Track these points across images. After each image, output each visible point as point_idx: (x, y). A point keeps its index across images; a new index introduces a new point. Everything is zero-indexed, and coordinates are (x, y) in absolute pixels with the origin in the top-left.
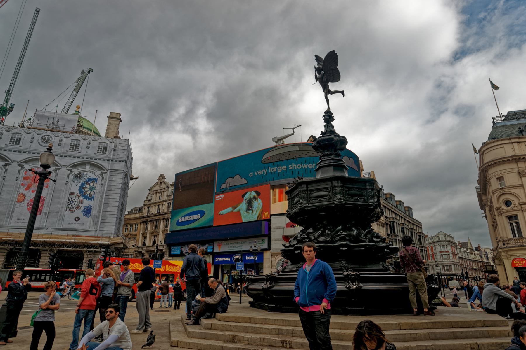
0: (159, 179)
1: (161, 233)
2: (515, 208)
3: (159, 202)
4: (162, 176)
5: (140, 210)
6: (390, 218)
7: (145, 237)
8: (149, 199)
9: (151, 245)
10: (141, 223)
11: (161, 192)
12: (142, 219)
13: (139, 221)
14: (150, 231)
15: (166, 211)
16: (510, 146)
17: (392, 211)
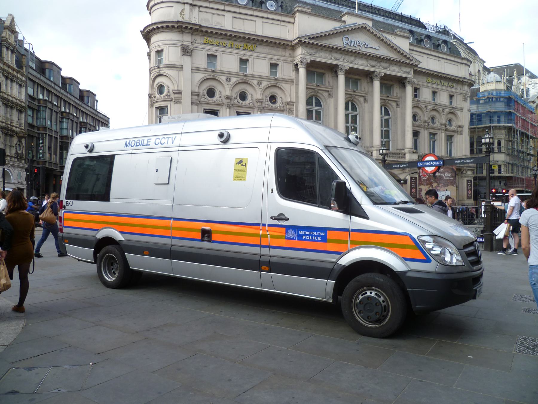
2: (166, 97)
6: (39, 100)
16: (181, 7)
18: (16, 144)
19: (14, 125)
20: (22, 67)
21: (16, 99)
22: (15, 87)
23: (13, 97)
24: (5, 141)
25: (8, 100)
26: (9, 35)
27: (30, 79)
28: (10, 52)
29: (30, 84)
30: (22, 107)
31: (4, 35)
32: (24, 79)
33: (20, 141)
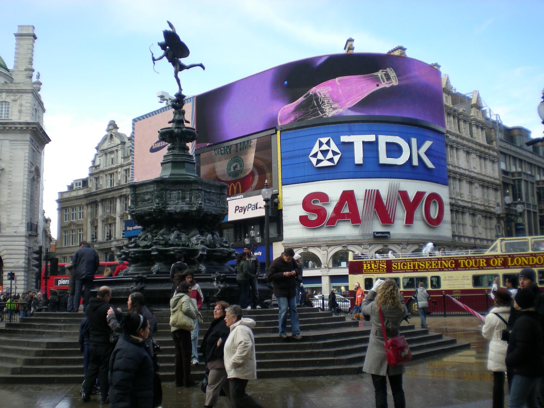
0: (108, 130)
1: (118, 220)
3: (111, 169)
4: (113, 125)
5: (85, 182)
6: (513, 174)
7: (96, 227)
8: (97, 163)
9: (105, 240)
10: (87, 205)
11: (112, 152)
12: (89, 198)
13: (84, 202)
14: (102, 216)
15: (123, 183)
17: (521, 161)
18: (496, 226)
19: (492, 205)
20: (492, 141)
21: (491, 178)
22: (489, 164)
23: (488, 177)
24: (486, 224)
25: (483, 181)
26: (477, 112)
27: (501, 153)
28: (480, 130)
29: (502, 157)
30: (498, 185)
31: (472, 114)
32: (495, 154)
33: (499, 222)
